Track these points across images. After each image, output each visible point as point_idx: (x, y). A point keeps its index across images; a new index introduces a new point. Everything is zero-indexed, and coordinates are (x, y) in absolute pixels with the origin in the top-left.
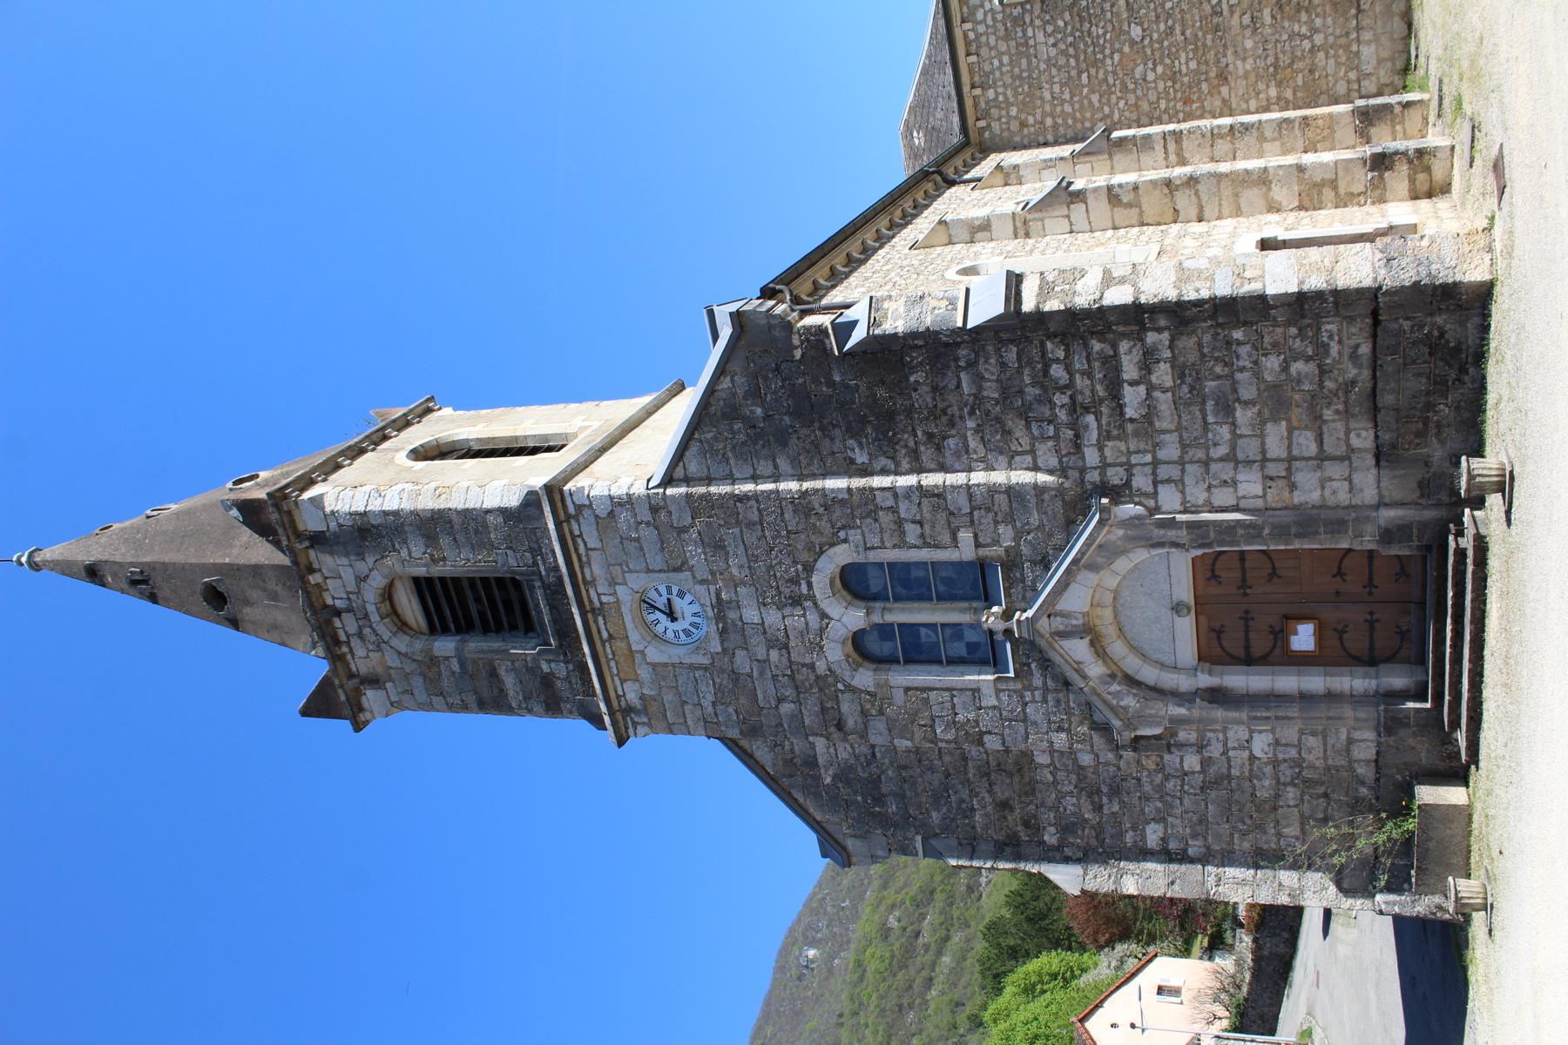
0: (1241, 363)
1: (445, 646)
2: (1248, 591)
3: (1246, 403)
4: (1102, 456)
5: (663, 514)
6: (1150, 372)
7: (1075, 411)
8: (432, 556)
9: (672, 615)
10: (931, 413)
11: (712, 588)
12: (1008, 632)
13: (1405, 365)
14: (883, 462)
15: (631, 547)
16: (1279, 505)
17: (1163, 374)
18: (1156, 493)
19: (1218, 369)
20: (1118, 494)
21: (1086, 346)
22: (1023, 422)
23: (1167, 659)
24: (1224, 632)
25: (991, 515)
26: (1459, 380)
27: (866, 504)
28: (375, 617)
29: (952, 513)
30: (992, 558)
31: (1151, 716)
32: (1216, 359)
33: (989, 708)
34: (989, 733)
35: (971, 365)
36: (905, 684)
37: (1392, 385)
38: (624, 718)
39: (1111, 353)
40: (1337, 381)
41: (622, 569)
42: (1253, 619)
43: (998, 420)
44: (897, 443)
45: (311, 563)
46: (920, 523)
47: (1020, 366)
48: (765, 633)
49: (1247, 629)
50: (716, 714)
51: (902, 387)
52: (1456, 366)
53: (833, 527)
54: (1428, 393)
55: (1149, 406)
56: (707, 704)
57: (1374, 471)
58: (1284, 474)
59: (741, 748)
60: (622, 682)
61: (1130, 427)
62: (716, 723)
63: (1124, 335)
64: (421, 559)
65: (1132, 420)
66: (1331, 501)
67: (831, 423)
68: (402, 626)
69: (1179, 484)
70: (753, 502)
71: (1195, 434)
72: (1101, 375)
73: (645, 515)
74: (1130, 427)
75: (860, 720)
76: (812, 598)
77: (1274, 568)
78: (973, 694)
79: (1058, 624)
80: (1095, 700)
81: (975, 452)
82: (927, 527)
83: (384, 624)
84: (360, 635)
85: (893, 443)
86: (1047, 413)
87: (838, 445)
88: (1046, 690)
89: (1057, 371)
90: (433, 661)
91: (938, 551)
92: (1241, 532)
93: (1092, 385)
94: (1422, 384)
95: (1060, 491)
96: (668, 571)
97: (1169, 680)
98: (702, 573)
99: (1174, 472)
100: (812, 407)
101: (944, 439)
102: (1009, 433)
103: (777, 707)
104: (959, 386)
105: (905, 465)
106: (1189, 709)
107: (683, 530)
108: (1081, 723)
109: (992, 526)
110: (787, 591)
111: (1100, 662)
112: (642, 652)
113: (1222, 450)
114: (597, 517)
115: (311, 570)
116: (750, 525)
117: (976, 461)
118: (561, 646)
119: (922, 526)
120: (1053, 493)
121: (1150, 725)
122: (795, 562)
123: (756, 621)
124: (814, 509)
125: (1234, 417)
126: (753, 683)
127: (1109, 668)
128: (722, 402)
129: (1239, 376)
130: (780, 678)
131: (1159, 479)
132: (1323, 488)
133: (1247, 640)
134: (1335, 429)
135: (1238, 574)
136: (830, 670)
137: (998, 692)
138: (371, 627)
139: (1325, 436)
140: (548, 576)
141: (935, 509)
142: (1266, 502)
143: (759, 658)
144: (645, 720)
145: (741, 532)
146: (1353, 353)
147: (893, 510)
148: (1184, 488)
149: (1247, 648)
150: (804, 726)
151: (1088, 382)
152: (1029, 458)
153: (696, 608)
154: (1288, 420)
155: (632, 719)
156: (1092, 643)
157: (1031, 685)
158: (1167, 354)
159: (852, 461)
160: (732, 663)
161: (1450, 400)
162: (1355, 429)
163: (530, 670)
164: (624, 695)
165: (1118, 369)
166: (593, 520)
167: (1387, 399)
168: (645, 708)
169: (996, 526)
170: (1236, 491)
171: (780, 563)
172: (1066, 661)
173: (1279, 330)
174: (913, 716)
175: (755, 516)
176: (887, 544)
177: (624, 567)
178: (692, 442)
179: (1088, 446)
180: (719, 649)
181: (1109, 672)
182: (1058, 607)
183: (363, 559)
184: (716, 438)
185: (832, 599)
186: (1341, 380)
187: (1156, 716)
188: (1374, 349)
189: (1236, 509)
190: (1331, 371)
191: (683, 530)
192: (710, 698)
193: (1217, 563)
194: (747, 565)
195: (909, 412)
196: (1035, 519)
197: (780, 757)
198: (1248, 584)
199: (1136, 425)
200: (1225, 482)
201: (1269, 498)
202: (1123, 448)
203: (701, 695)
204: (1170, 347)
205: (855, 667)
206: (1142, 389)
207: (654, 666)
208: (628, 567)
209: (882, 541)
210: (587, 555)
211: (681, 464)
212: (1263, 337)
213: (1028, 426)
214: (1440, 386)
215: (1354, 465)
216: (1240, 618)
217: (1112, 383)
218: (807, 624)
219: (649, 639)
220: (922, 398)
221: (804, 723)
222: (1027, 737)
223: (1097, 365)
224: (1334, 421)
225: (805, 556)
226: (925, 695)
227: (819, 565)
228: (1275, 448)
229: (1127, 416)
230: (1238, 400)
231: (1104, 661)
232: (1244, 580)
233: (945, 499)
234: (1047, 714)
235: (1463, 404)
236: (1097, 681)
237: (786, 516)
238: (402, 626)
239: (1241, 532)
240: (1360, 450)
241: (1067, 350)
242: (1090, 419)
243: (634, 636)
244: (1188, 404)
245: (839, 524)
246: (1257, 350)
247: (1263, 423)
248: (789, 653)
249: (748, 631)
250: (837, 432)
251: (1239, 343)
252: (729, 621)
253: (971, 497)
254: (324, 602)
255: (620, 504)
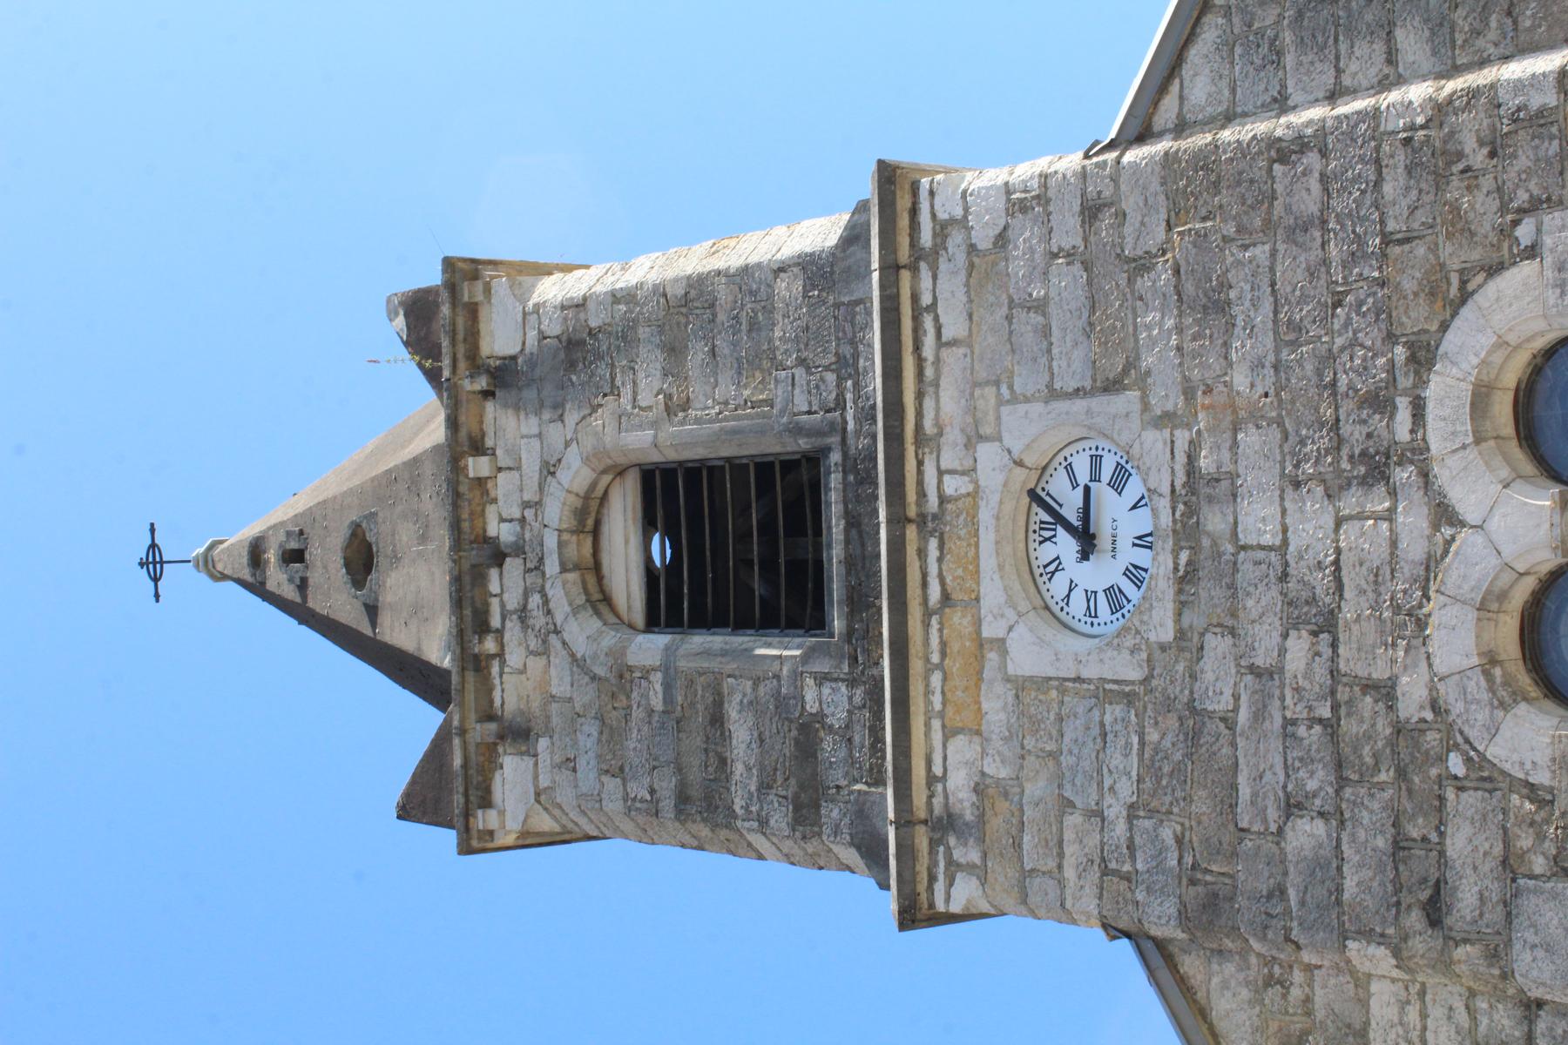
1: (649, 648)
5: (1106, 219)
8: (669, 397)
9: (1087, 540)
11: (1182, 437)
15: (1027, 322)
28: (552, 566)
38: (932, 845)
41: (999, 394)
45: (483, 435)
48: (1284, 577)
50: (1131, 847)
53: (1503, 209)
56: (1115, 810)
59: (1182, 982)
60: (949, 734)
62: (1127, 878)
64: (650, 408)
68: (600, 600)
70: (1312, 159)
73: (1068, 231)
75: (1495, 891)
76: (1418, 454)
83: (564, 584)
84: (523, 613)
90: (624, 677)
98: (1165, 396)
103: (1280, 831)
107: (1141, 265)
112: (1001, 644)
114: (972, 248)
115: (478, 447)
118: (849, 634)
122: (1391, 338)
123: (1267, 539)
124: (1460, 155)
126: (1234, 745)
130: (1302, 731)
136: (1435, 706)
138: (543, 592)
140: (858, 433)
143: (1259, 662)
144: (974, 856)
145: (1273, 253)
150: (1339, 902)
153: (1142, 522)
155: (948, 850)
160: (1193, 677)
163: (781, 702)
164: (944, 778)
166: (961, 258)
168: (981, 818)
171: (1354, 343)
175: (1309, 201)
177: (1004, 390)
178: (1208, 19)
180: (1167, 634)
183: (561, 418)
185: (1472, 453)
191: (1141, 265)
192: (1126, 790)
194: (1271, 358)
197: (1273, 1027)
203: (1107, 783)
207: (1022, 686)
208: (1011, 387)
210: (937, 360)
211: (1175, 88)
218: (1394, 543)
219: (1024, 606)
221: (1339, 889)
225: (1416, 317)
227: (1451, 342)
237: (1388, 188)
238: (600, 600)
243: (992, 592)
245: (1522, 197)
248: (1334, 645)
249: (1248, 571)
252: (1206, 542)
254: (485, 531)
255: (1023, 207)
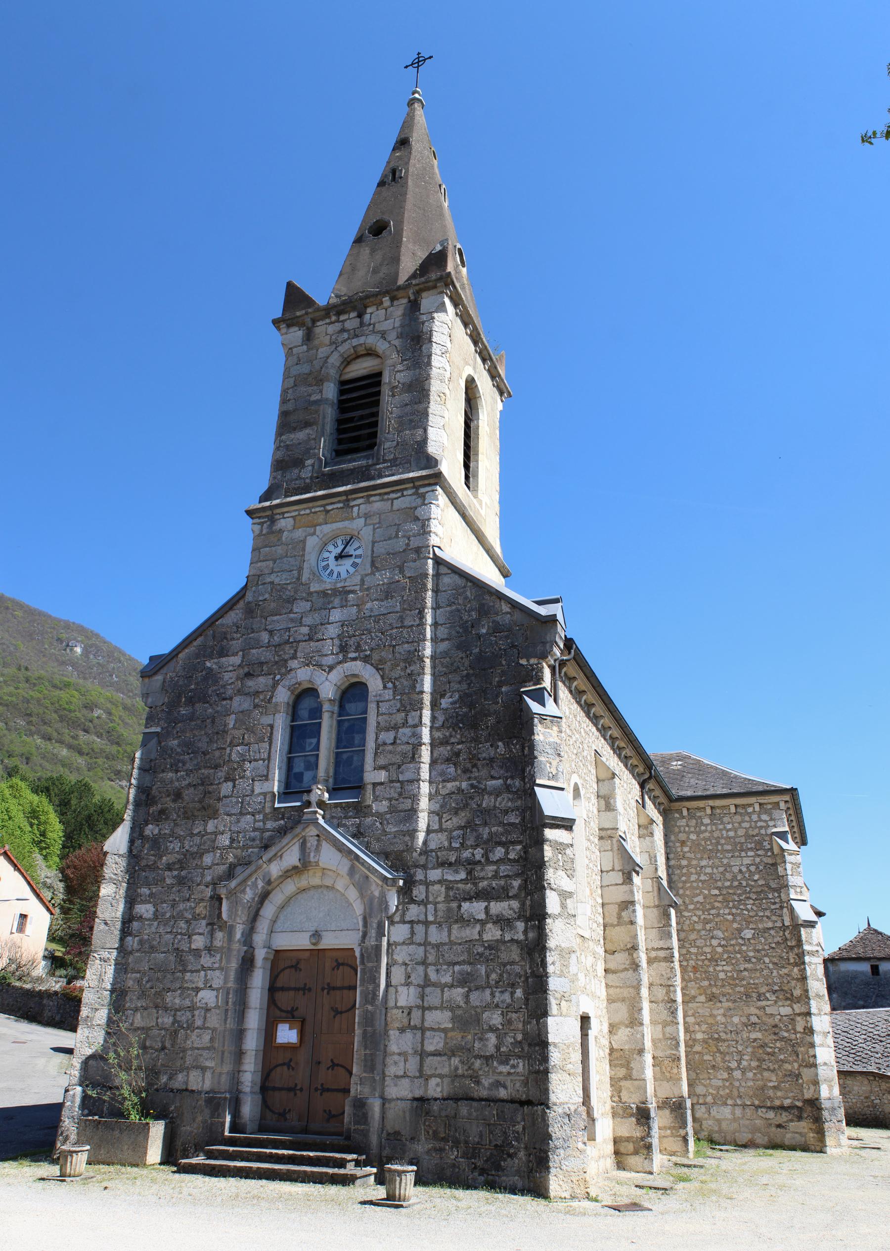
0: (497, 994)
2: (326, 991)
3: (467, 996)
4: (434, 883)
6: (494, 923)
7: (469, 864)
10: (474, 756)
11: (357, 588)
12: (308, 804)
13: (489, 1125)
14: (441, 719)
16: (389, 1019)
17: (492, 933)
18: (404, 922)
19: (494, 976)
20: (406, 893)
21: (517, 875)
22: (463, 824)
23: (278, 926)
24: (296, 970)
25: (396, 796)
26: (475, 1168)
27: (411, 704)
29: (399, 766)
30: (364, 795)
31: (237, 911)
32: (501, 975)
33: (253, 788)
34: (234, 786)
35: (508, 788)
36: (276, 725)
37: (475, 1114)
39: (510, 894)
40: (480, 1069)
42: (304, 994)
43: (466, 805)
44: (454, 729)
46: (394, 743)
47: (504, 825)
48: (322, 624)
49: (297, 989)
51: (494, 736)
52: (486, 1166)
53: (396, 679)
54: (466, 1142)
55: (470, 921)
57: (410, 1096)
58: (412, 1024)
61: (454, 905)
63: (523, 904)
65: (460, 907)
66: (389, 1060)
67: (472, 682)
69: (410, 942)
71: (447, 955)
72: (494, 885)
73: (414, 543)
74: (454, 905)
76: (344, 661)
77: (341, 1013)
78: (264, 776)
79: (312, 842)
80: (252, 868)
81: (443, 787)
82: (390, 748)
85: (455, 727)
86: (469, 843)
87: (456, 686)
88: (263, 831)
89: (499, 852)
91: (373, 755)
92: (371, 987)
93: (488, 878)
94: (474, 1138)
95: (410, 849)
96: (372, 557)
97: (263, 926)
99: (419, 938)
100: (484, 670)
101: (455, 765)
102: (456, 813)
104: (493, 778)
105: (438, 734)
106: (239, 941)
108: (235, 857)
109: (388, 796)
110: (351, 643)
111: (280, 873)
113: (433, 976)
116: (402, 619)
117: (437, 787)
119: (392, 744)
120: (409, 844)
121: (230, 910)
125: (457, 986)
127: (276, 880)
128: (492, 604)
129: (488, 992)
131: (415, 925)
132: (400, 1054)
133: (289, 989)
134: (442, 1065)
135: (339, 984)
136: (291, 670)
137: (264, 794)
139: (439, 1058)
141: (404, 755)
142: (392, 1008)
145: (397, 612)
146: (500, 1084)
147: (405, 724)
148: (407, 944)
149: (282, 989)
151: (490, 876)
152: (436, 827)
154: (452, 1029)
156: (295, 868)
157: (268, 819)
158: (507, 937)
159: (443, 696)
161: (461, 1160)
162: (442, 1082)
165: (498, 899)
167: (464, 1109)
169: (387, 799)
170: (402, 985)
172: (284, 847)
173: (520, 1026)
174: (251, 730)
175: (408, 622)
176: (380, 718)
178: (464, 581)
179: (442, 873)
181: (272, 880)
182: (324, 844)
184: (466, 598)
185: (343, 675)
186: (481, 1073)
187: (236, 915)
188: (503, 1101)
189: (388, 984)
190: (488, 1065)
193: (349, 968)
195: (476, 740)
196: (392, 829)
198: (331, 992)
199: (456, 909)
200: (409, 977)
201: (395, 1011)
202: (440, 899)
204: (512, 940)
205: (291, 689)
206: (482, 916)
209: (383, 714)
211: (449, 571)
212: (516, 1012)
213: (460, 828)
214: (471, 1153)
215: (416, 1080)
216: (305, 984)
217: (488, 893)
220: (486, 751)
222: (228, 815)
223: (502, 882)
224: (450, 1065)
226: (266, 739)
227: (369, 667)
228: (435, 1018)
229: (463, 904)
230: (470, 990)
231: (281, 876)
232: (334, 988)
233: (410, 762)
234: (245, 831)
235: (457, 1170)
236: (267, 870)
237: (406, 645)
239: (371, 987)
240: (426, 1085)
241: (514, 861)
242: (463, 875)
244: (469, 951)
245: (397, 683)
246: (507, 1007)
247: (452, 1009)
250: (464, 686)
251: (512, 994)
253: (411, 781)
